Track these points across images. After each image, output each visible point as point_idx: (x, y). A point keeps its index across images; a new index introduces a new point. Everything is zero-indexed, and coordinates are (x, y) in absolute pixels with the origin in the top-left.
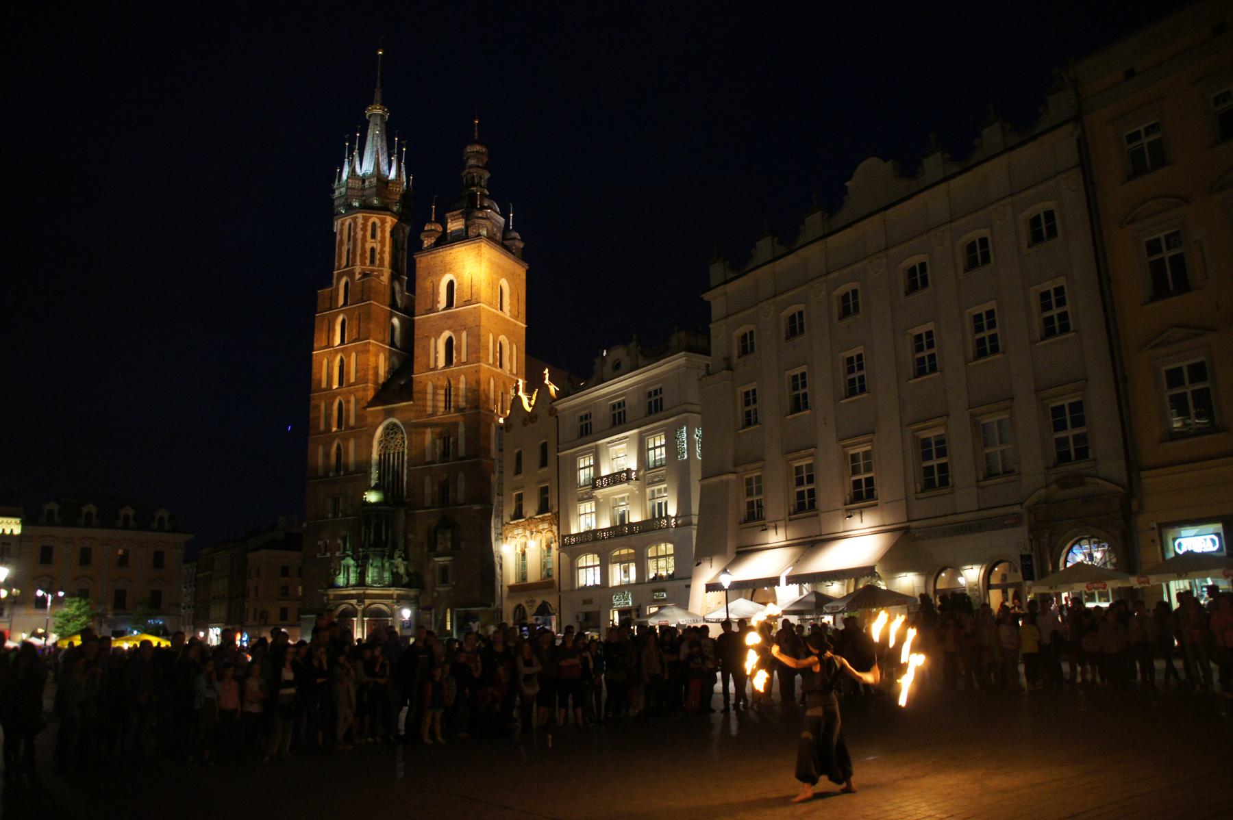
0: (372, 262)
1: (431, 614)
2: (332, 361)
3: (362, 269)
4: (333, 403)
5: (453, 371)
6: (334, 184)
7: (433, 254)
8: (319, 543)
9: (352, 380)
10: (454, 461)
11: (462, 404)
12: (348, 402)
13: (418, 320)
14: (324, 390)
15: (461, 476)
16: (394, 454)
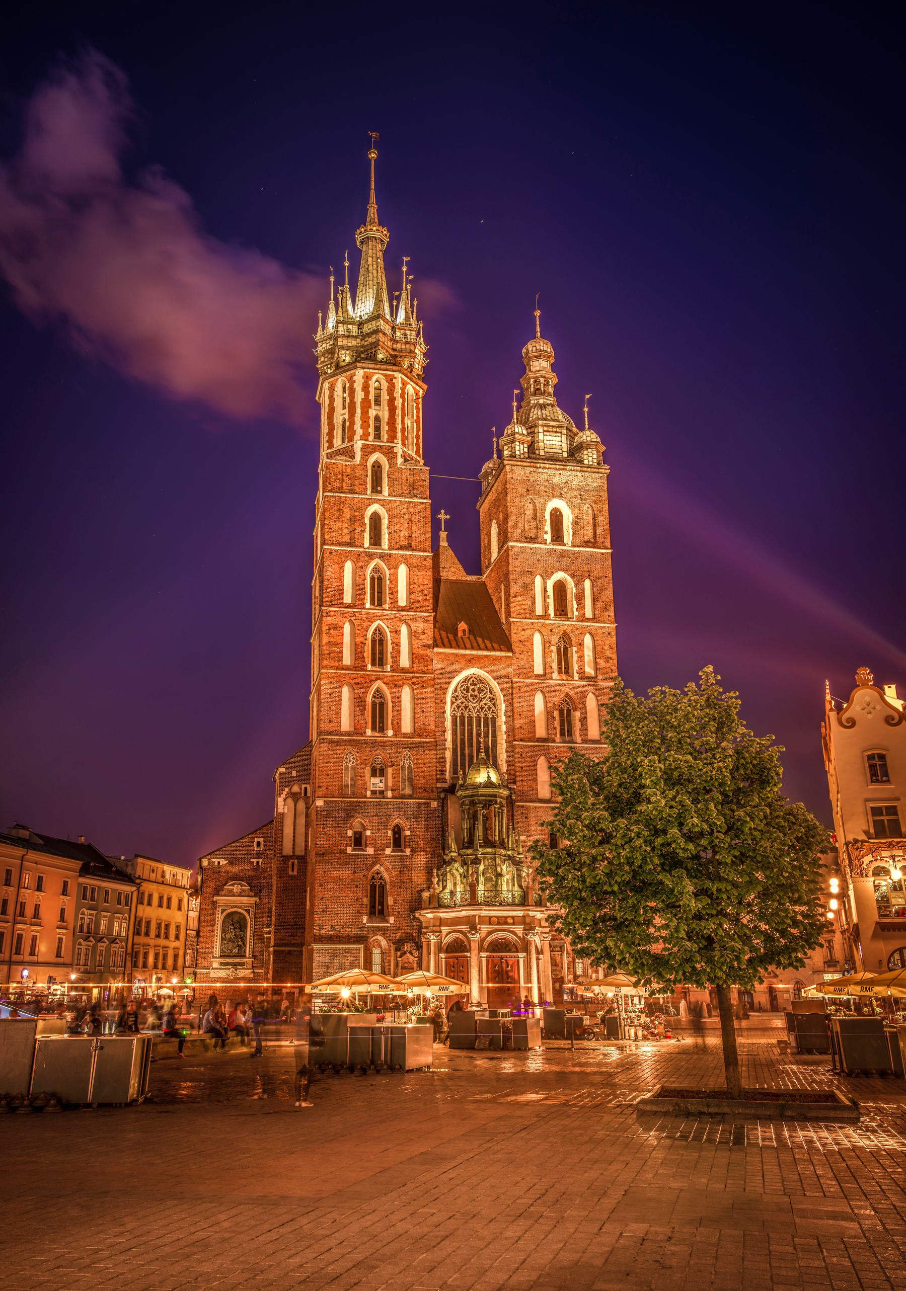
7: (536, 467)
10: (582, 743)
12: (397, 632)
13: (513, 547)
14: (348, 606)
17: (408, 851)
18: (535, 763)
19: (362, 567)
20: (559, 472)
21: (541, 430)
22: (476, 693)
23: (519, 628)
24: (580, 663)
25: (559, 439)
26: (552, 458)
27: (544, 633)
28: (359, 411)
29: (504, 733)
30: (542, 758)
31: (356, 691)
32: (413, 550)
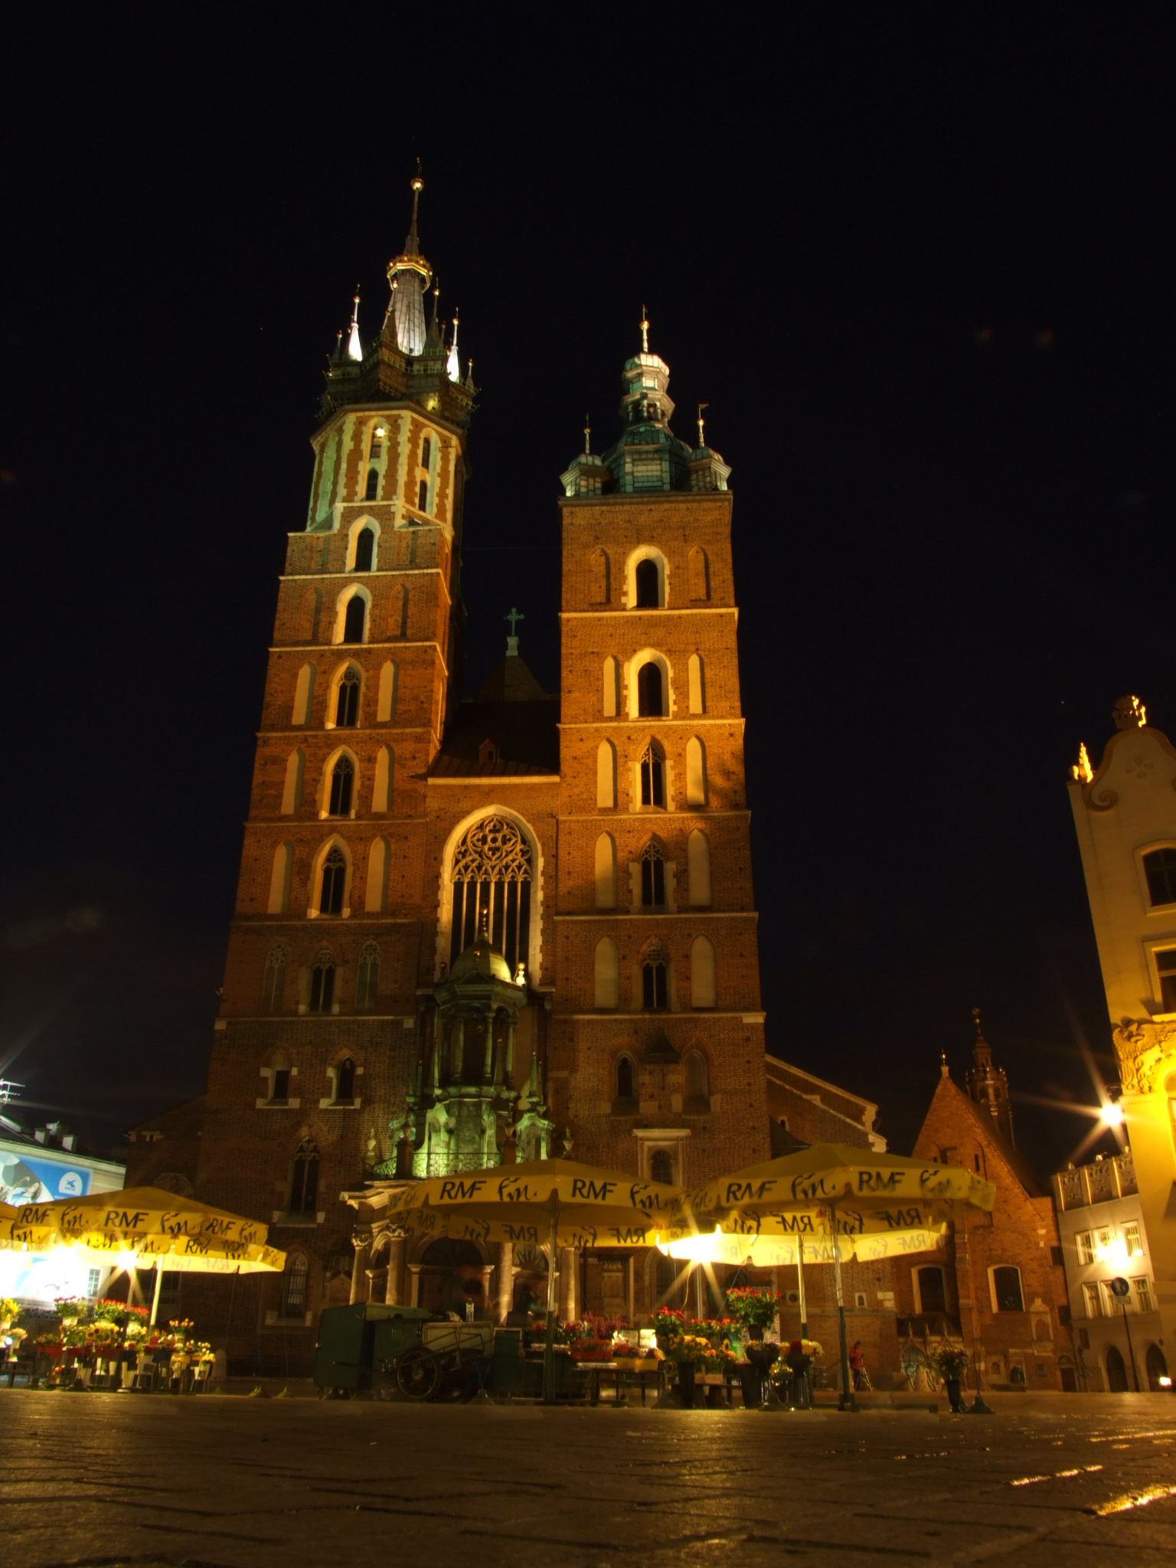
0: (422, 507)
1: (626, 1271)
2: (328, 673)
3: (408, 511)
4: (323, 760)
5: (670, 728)
6: (331, 355)
8: (266, 1073)
9: (384, 714)
10: (679, 912)
11: (695, 793)
12: (371, 760)
13: (568, 620)
14: (299, 728)
15: (701, 947)
16: (499, 886)
17: (358, 1103)
18: (591, 950)
19: (325, 672)
20: (649, 507)
21: (628, 460)
22: (499, 843)
23: (574, 738)
24: (678, 784)
25: (659, 467)
26: (649, 492)
27: (616, 743)
28: (344, 466)
29: (539, 904)
30: (606, 940)
31: (297, 852)
32: (408, 640)
